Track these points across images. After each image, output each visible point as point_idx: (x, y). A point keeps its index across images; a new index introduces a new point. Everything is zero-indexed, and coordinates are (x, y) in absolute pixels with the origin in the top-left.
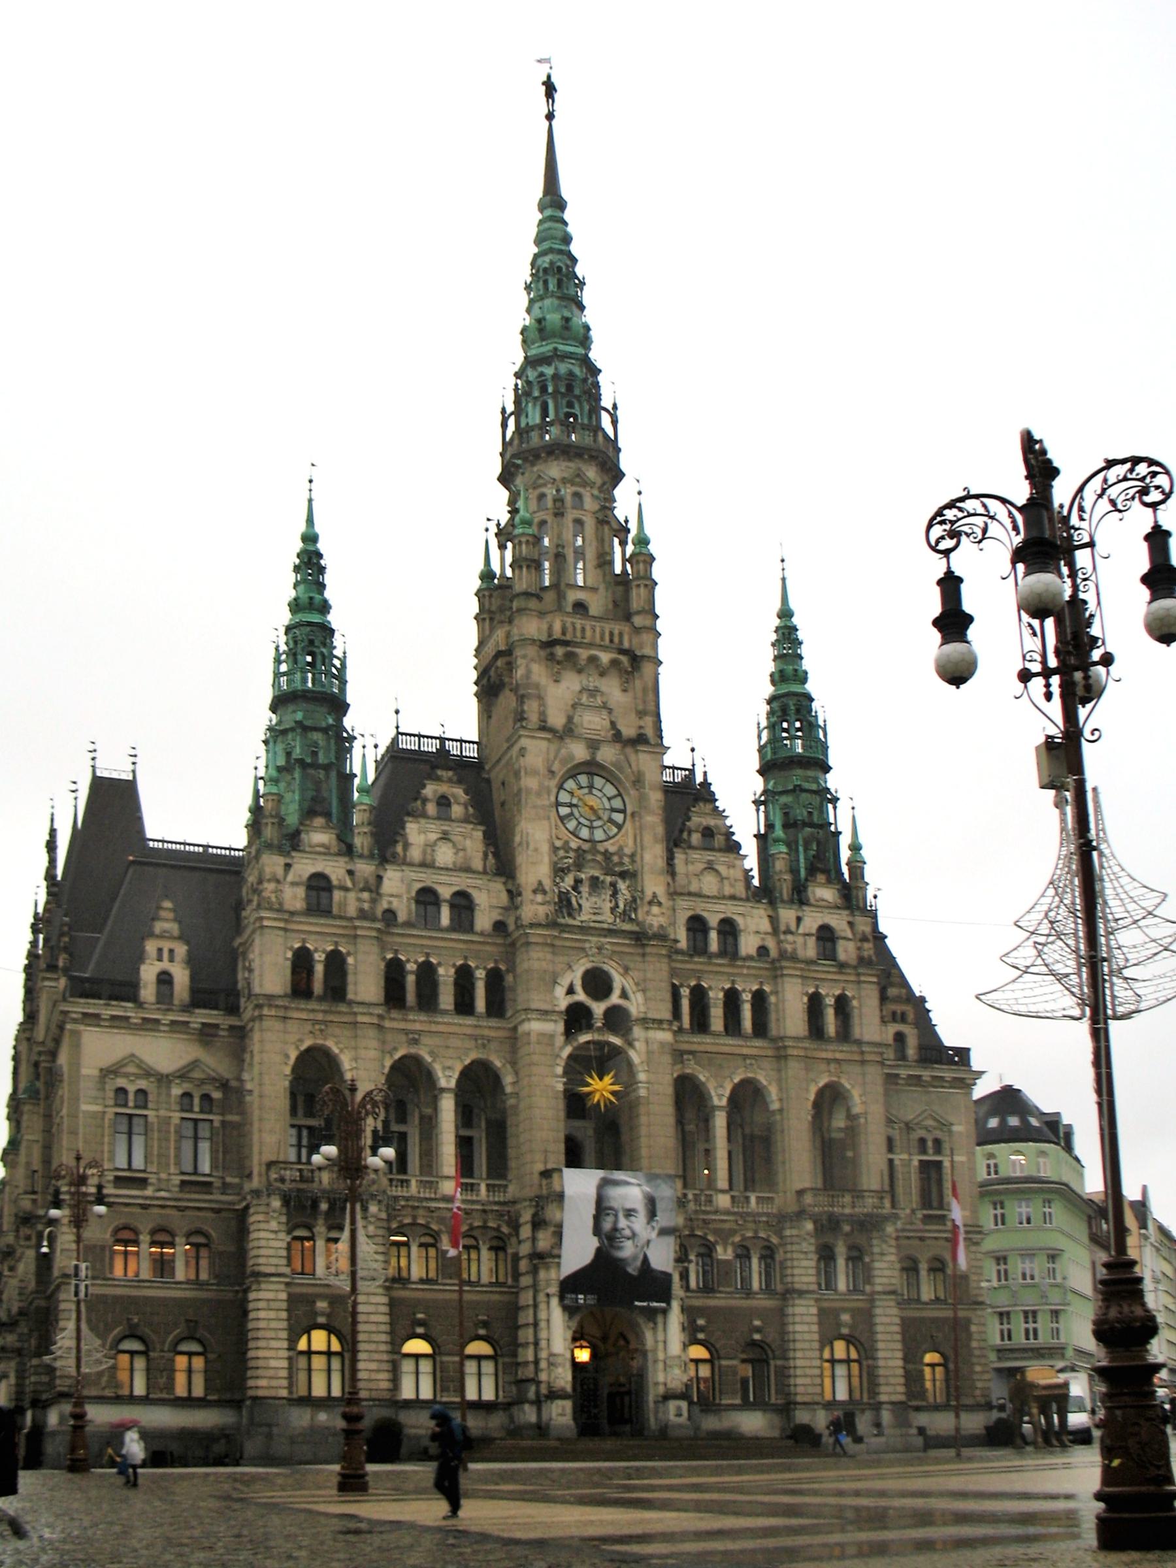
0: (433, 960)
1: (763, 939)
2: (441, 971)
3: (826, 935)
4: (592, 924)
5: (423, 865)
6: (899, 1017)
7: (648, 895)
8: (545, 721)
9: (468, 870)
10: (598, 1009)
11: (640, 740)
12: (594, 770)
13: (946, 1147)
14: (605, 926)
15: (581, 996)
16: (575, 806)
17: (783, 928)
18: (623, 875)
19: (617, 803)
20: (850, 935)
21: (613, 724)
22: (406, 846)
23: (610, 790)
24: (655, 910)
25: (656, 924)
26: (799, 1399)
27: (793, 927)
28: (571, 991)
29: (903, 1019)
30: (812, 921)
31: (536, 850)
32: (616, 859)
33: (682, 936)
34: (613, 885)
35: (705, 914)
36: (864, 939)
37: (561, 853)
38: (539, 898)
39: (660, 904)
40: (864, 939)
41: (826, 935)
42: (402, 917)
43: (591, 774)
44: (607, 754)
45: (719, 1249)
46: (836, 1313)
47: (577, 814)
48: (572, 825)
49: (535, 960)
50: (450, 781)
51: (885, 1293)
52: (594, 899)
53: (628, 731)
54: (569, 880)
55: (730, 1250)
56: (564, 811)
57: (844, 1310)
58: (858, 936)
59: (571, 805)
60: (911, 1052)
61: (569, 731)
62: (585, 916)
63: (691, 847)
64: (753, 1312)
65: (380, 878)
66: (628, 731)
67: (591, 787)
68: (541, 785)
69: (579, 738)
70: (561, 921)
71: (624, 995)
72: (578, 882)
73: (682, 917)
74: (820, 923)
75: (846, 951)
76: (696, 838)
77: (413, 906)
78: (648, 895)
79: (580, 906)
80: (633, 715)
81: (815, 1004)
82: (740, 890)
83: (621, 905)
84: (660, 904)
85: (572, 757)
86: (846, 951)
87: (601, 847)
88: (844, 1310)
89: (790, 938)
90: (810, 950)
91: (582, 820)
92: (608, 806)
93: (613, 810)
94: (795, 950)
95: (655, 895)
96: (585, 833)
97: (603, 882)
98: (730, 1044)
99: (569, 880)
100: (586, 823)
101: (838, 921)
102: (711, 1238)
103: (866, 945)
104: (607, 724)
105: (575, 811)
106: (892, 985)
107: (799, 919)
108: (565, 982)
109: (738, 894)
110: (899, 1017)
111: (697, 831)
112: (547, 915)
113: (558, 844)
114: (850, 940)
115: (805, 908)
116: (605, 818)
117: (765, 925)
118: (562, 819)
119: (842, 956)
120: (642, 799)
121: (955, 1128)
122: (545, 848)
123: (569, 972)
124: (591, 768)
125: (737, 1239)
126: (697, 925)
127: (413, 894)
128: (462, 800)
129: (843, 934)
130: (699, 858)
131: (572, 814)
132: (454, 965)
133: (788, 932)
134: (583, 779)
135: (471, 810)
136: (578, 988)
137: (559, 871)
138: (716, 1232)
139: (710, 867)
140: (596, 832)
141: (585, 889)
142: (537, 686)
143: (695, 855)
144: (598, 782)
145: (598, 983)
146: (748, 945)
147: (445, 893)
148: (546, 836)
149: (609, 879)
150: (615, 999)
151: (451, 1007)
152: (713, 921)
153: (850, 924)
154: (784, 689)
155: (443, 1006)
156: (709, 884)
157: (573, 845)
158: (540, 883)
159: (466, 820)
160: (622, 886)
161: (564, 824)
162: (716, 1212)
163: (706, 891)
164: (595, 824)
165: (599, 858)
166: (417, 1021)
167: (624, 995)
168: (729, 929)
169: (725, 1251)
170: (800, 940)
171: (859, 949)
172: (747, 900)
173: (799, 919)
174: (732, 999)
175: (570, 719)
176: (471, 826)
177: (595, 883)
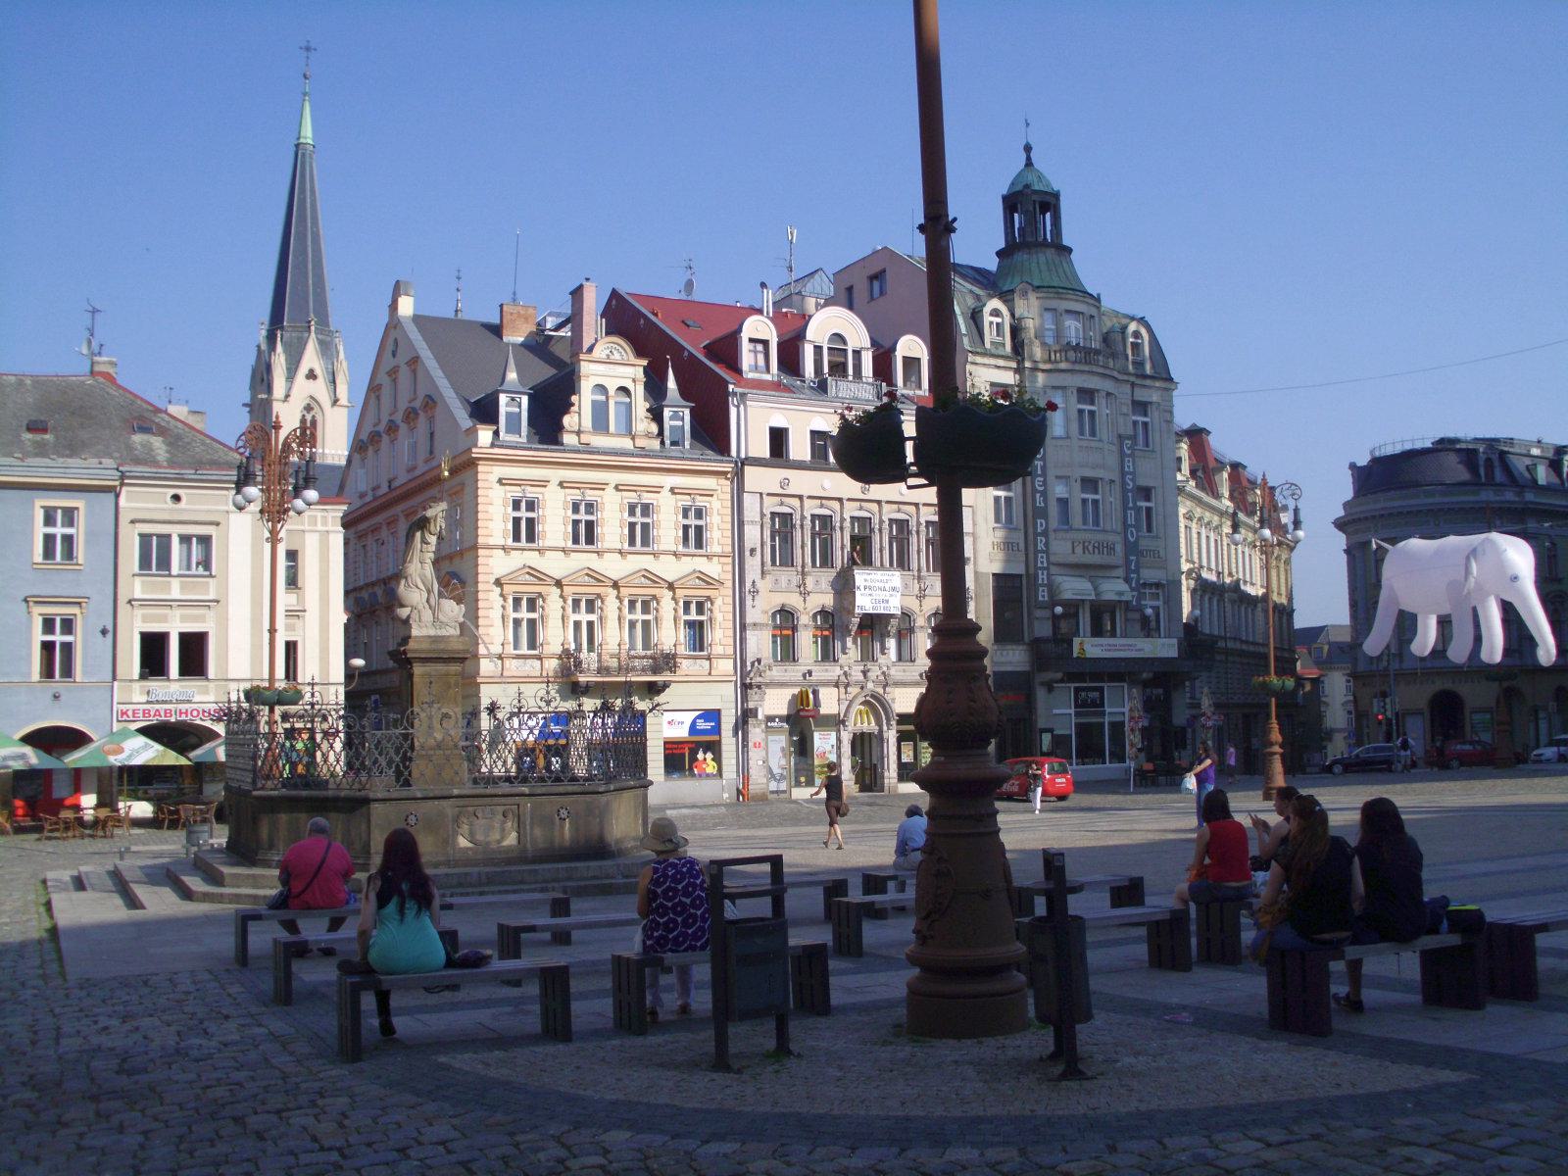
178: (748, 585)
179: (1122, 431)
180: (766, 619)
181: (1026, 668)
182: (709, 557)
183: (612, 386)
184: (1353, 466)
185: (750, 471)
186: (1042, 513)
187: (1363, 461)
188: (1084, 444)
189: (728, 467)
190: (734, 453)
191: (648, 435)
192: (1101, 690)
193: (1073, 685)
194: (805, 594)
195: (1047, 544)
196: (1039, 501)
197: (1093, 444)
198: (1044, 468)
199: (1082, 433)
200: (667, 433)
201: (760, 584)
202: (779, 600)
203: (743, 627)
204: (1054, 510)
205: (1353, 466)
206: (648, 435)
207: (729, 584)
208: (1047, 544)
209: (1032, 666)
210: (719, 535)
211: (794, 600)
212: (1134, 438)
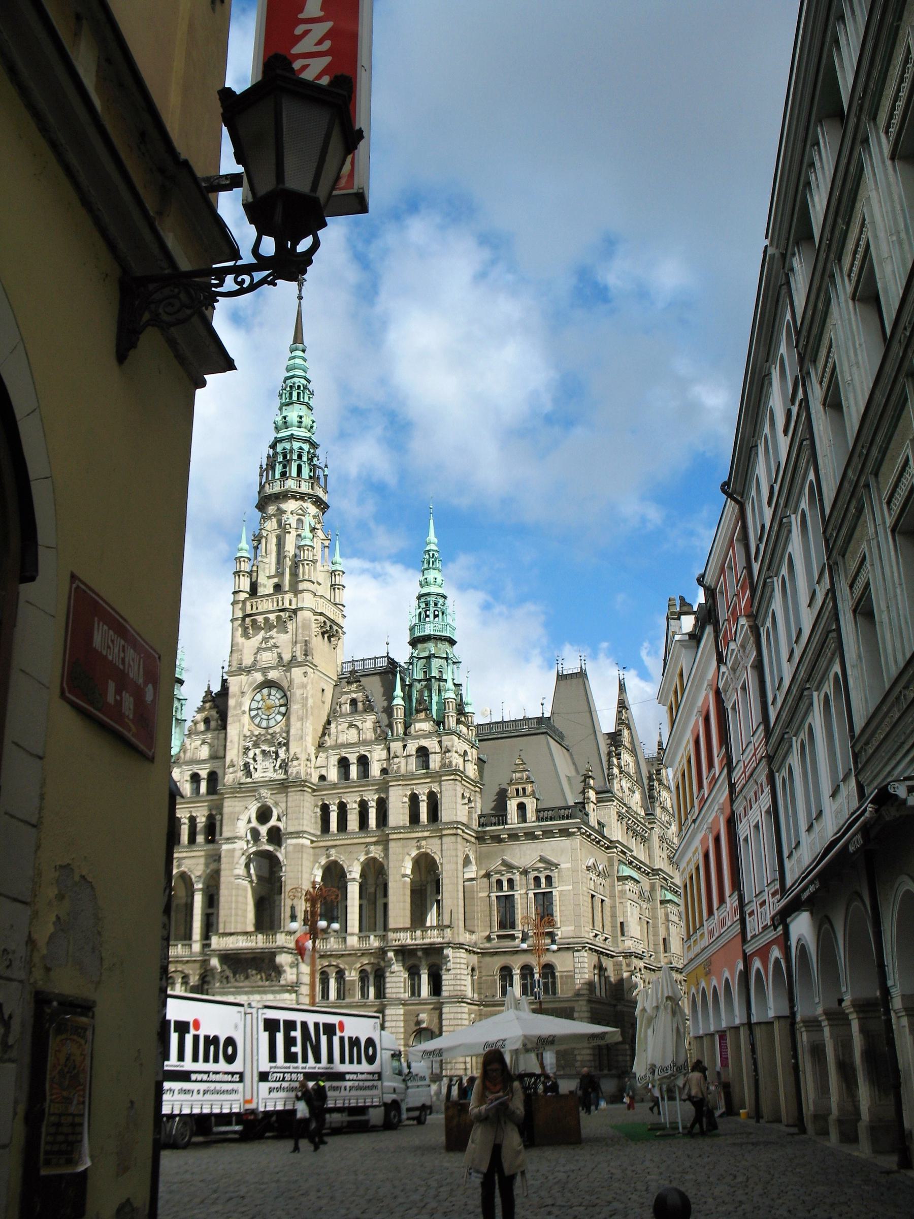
0: (194, 814)
2: (198, 820)
3: (423, 753)
4: (259, 780)
10: (263, 830)
11: (294, 657)
12: (271, 684)
13: (555, 880)
14: (267, 779)
15: (254, 823)
16: (260, 708)
17: (392, 755)
20: (438, 750)
25: (295, 772)
28: (249, 821)
30: (412, 747)
31: (231, 741)
33: (333, 775)
34: (277, 753)
35: (347, 755)
37: (248, 739)
41: (423, 753)
43: (270, 687)
44: (273, 675)
47: (260, 714)
48: (257, 721)
49: (230, 806)
52: (264, 763)
54: (251, 754)
56: (253, 713)
58: (443, 750)
59: (258, 709)
60: (531, 815)
62: (257, 776)
66: (287, 657)
67: (269, 695)
68: (237, 701)
73: (334, 760)
74: (417, 746)
79: (256, 769)
81: (414, 799)
82: (370, 735)
83: (278, 765)
85: (256, 681)
87: (271, 731)
89: (396, 760)
94: (399, 767)
95: (295, 754)
96: (264, 724)
97: (269, 752)
99: (251, 754)
100: (266, 717)
101: (431, 744)
104: (275, 655)
105: (260, 711)
107: (405, 746)
108: (244, 818)
112: (234, 779)
114: (435, 753)
116: (276, 712)
117: (384, 755)
118: (252, 718)
121: (563, 866)
122: (236, 739)
123: (247, 810)
124: (269, 684)
126: (344, 763)
128: (215, 718)
129: (433, 750)
131: (257, 714)
132: (204, 816)
134: (265, 691)
135: (219, 722)
136: (254, 819)
139: (351, 725)
140: (270, 721)
141: (259, 758)
144: (273, 692)
145: (264, 815)
149: (273, 749)
150: (273, 822)
152: (353, 758)
153: (440, 742)
154: (425, 590)
156: (352, 736)
157: (256, 733)
161: (253, 722)
164: (270, 717)
165: (269, 737)
167: (279, 819)
168: (363, 761)
170: (403, 761)
173: (405, 746)
174: (363, 807)
176: (217, 732)
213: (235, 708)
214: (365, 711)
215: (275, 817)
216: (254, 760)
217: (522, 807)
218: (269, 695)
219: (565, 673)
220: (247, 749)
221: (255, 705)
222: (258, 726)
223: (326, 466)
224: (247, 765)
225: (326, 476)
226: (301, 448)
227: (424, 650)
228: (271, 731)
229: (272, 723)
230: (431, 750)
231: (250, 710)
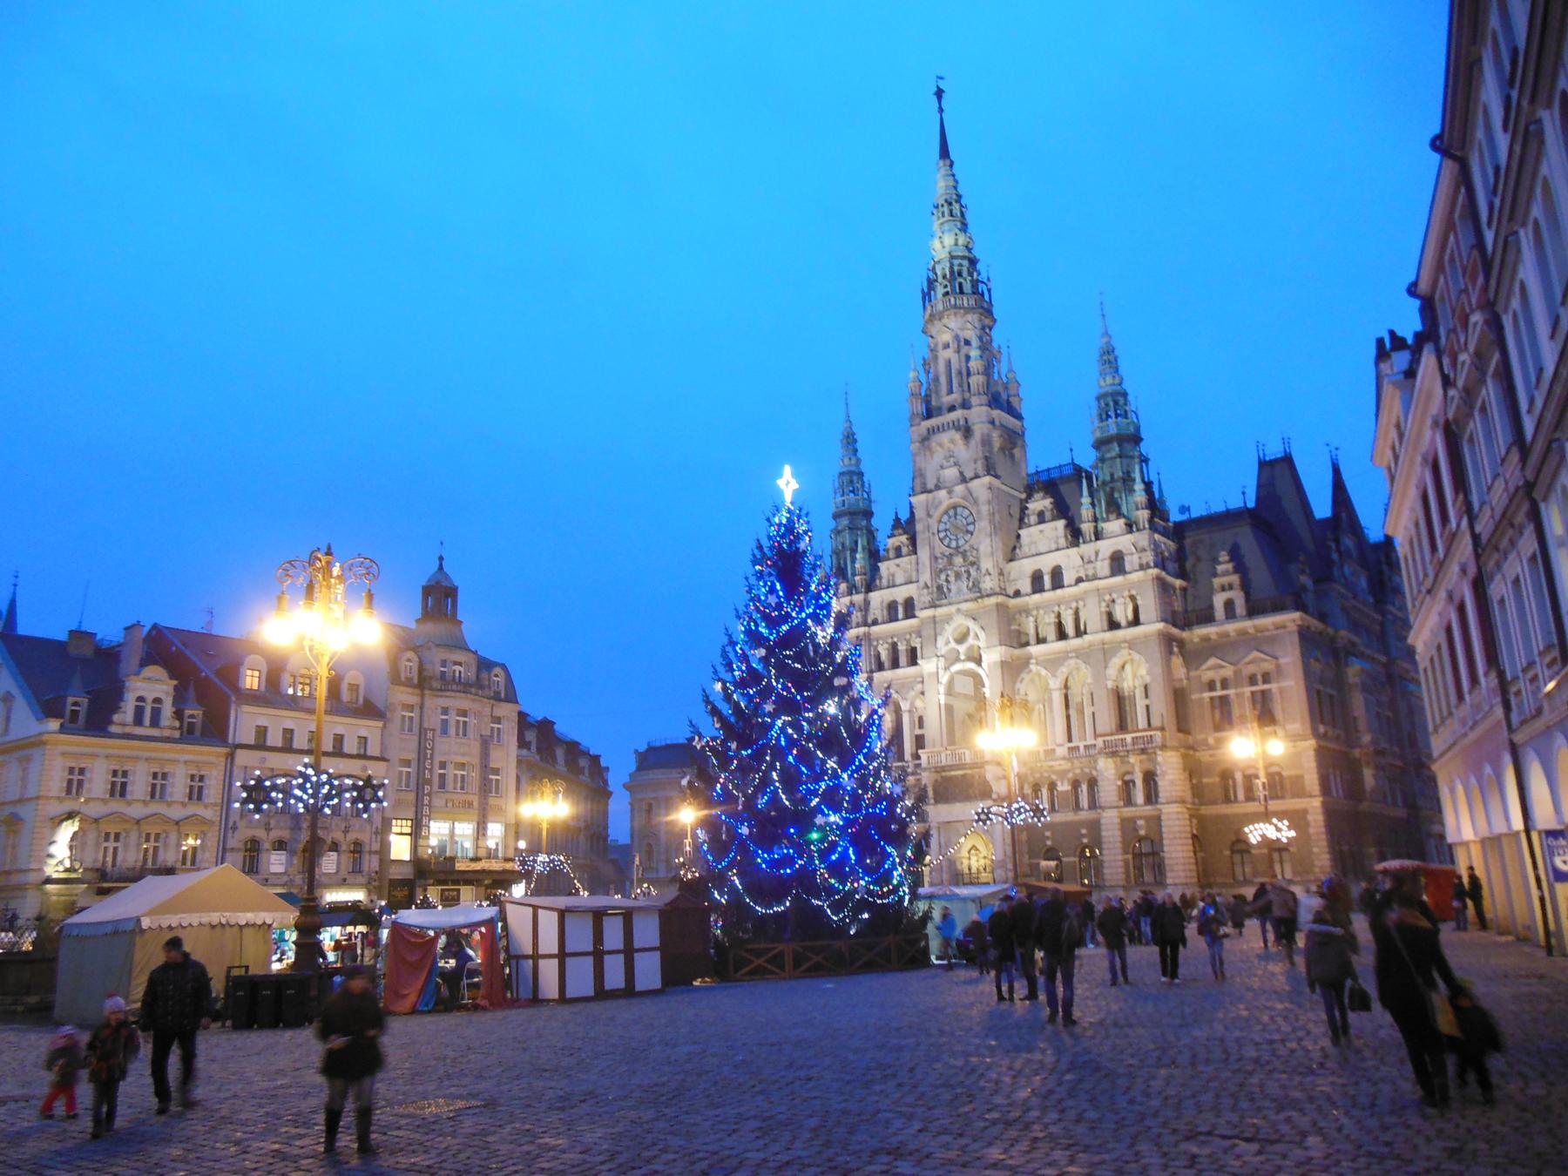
1: (1077, 572)
5: (888, 587)
6: (1227, 587)
7: (984, 571)
8: (925, 487)
9: (911, 582)
15: (953, 644)
18: (972, 564)
19: (970, 519)
20: (1134, 550)
21: (961, 473)
22: (881, 578)
23: (966, 513)
24: (988, 578)
25: (988, 588)
26: (1107, 884)
27: (1093, 559)
28: (948, 643)
29: (1231, 587)
30: (1106, 547)
32: (969, 554)
33: (1026, 586)
34: (968, 572)
36: (1144, 550)
37: (940, 561)
38: (925, 591)
39: (990, 574)
40: (1144, 550)
42: (880, 620)
45: (1059, 783)
46: (1133, 820)
48: (946, 542)
50: (900, 535)
51: (1168, 803)
53: (969, 474)
54: (943, 577)
55: (1066, 783)
56: (942, 535)
57: (1141, 818)
59: (946, 530)
61: (938, 487)
62: (953, 596)
63: (1030, 526)
64: (1082, 823)
65: (867, 603)
67: (956, 514)
69: (945, 488)
70: (938, 603)
71: (977, 636)
72: (948, 576)
75: (1131, 563)
76: (1033, 519)
77: (885, 612)
78: (984, 571)
79: (949, 590)
80: (973, 465)
82: (1062, 542)
84: (990, 574)
86: (1131, 561)
87: (961, 550)
88: (1141, 818)
89: (1091, 566)
90: (1103, 567)
91: (952, 537)
92: (965, 522)
93: (968, 524)
96: (954, 544)
98: (1062, 644)
99: (943, 577)
102: (1054, 777)
103: (1143, 554)
106: (1220, 563)
109: (1061, 547)
110: (1227, 587)
111: (1034, 514)
113: (939, 555)
114: (1132, 554)
115: (1098, 542)
118: (941, 540)
119: (1128, 568)
120: (979, 512)
122: (927, 563)
125: (1070, 775)
127: (885, 604)
130: (1034, 530)
131: (947, 536)
133: (1090, 562)
137: (936, 573)
138: (1055, 773)
141: (952, 579)
142: (920, 470)
143: (1032, 529)
146: (1068, 577)
147: (900, 600)
148: (928, 554)
151: (905, 664)
155: (901, 664)
157: (947, 554)
158: (926, 584)
159: (909, 555)
160: (971, 571)
162: (1056, 760)
163: (1042, 551)
166: (888, 675)
168: (1057, 574)
169: (1062, 784)
171: (1140, 558)
172: (1068, 548)
175: (938, 479)
177: (958, 576)
178: (231, 824)
179: (483, 733)
180: (241, 845)
181: (411, 877)
182: (206, 806)
183: (150, 697)
184: (636, 751)
185: (239, 752)
186: (429, 782)
187: (643, 748)
188: (458, 741)
189: (224, 750)
190: (230, 741)
191: (174, 728)
192: (458, 890)
193: (440, 888)
194: (268, 829)
195: (430, 802)
196: (427, 776)
197: (463, 741)
198: (432, 755)
199: (457, 734)
200: (185, 725)
201: (238, 824)
202: (250, 833)
203: (224, 850)
204: (436, 780)
205: (636, 751)
206: (174, 728)
207: (218, 823)
208: (430, 802)
209: (415, 875)
210: (213, 791)
211: (260, 833)
212: (492, 736)
213: (923, 532)
214: (1053, 519)
215: (972, 634)
216: (947, 581)
217: (1229, 605)
218: (956, 514)
219: (1267, 459)
220: (941, 571)
221: (942, 527)
222: (948, 546)
223: (989, 279)
224: (940, 588)
225: (989, 290)
226: (960, 265)
227: (1109, 451)
228: (961, 550)
229: (961, 542)
230: (1124, 551)
231: (938, 532)
